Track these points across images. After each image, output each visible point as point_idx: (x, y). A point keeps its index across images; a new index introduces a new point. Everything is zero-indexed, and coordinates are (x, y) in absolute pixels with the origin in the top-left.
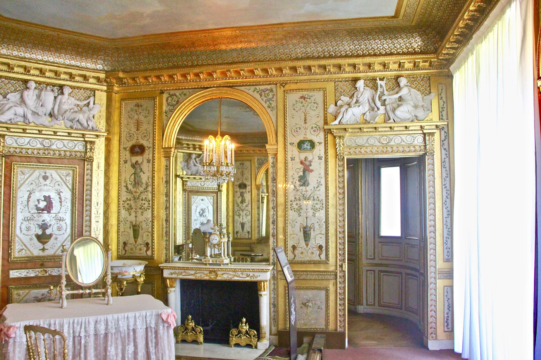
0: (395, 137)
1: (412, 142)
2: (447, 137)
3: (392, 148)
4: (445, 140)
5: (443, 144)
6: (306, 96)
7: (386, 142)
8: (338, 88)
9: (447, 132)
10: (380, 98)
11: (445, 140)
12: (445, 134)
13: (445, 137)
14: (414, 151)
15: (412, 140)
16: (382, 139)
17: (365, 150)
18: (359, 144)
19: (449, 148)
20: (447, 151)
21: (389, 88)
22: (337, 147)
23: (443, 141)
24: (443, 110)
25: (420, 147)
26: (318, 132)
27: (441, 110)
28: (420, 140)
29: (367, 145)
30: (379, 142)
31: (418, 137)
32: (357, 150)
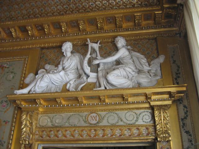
0: (109, 115)
1: (133, 121)
2: (188, 113)
3: (103, 130)
4: (185, 118)
5: (184, 124)
6: (5, 65)
7: (94, 122)
8: (43, 56)
9: (187, 105)
10: (90, 63)
11: (185, 118)
12: (185, 109)
13: (186, 113)
14: (139, 135)
15: (135, 119)
16: (90, 116)
17: (64, 133)
18: (56, 125)
19: (194, 131)
20: (190, 135)
21: (105, 53)
22: (23, 126)
23: (182, 120)
24: (179, 77)
25: (147, 129)
26: (8, 108)
27: (175, 76)
28: (147, 117)
29: (67, 124)
30: (85, 122)
31: (144, 114)
32: (52, 132)
